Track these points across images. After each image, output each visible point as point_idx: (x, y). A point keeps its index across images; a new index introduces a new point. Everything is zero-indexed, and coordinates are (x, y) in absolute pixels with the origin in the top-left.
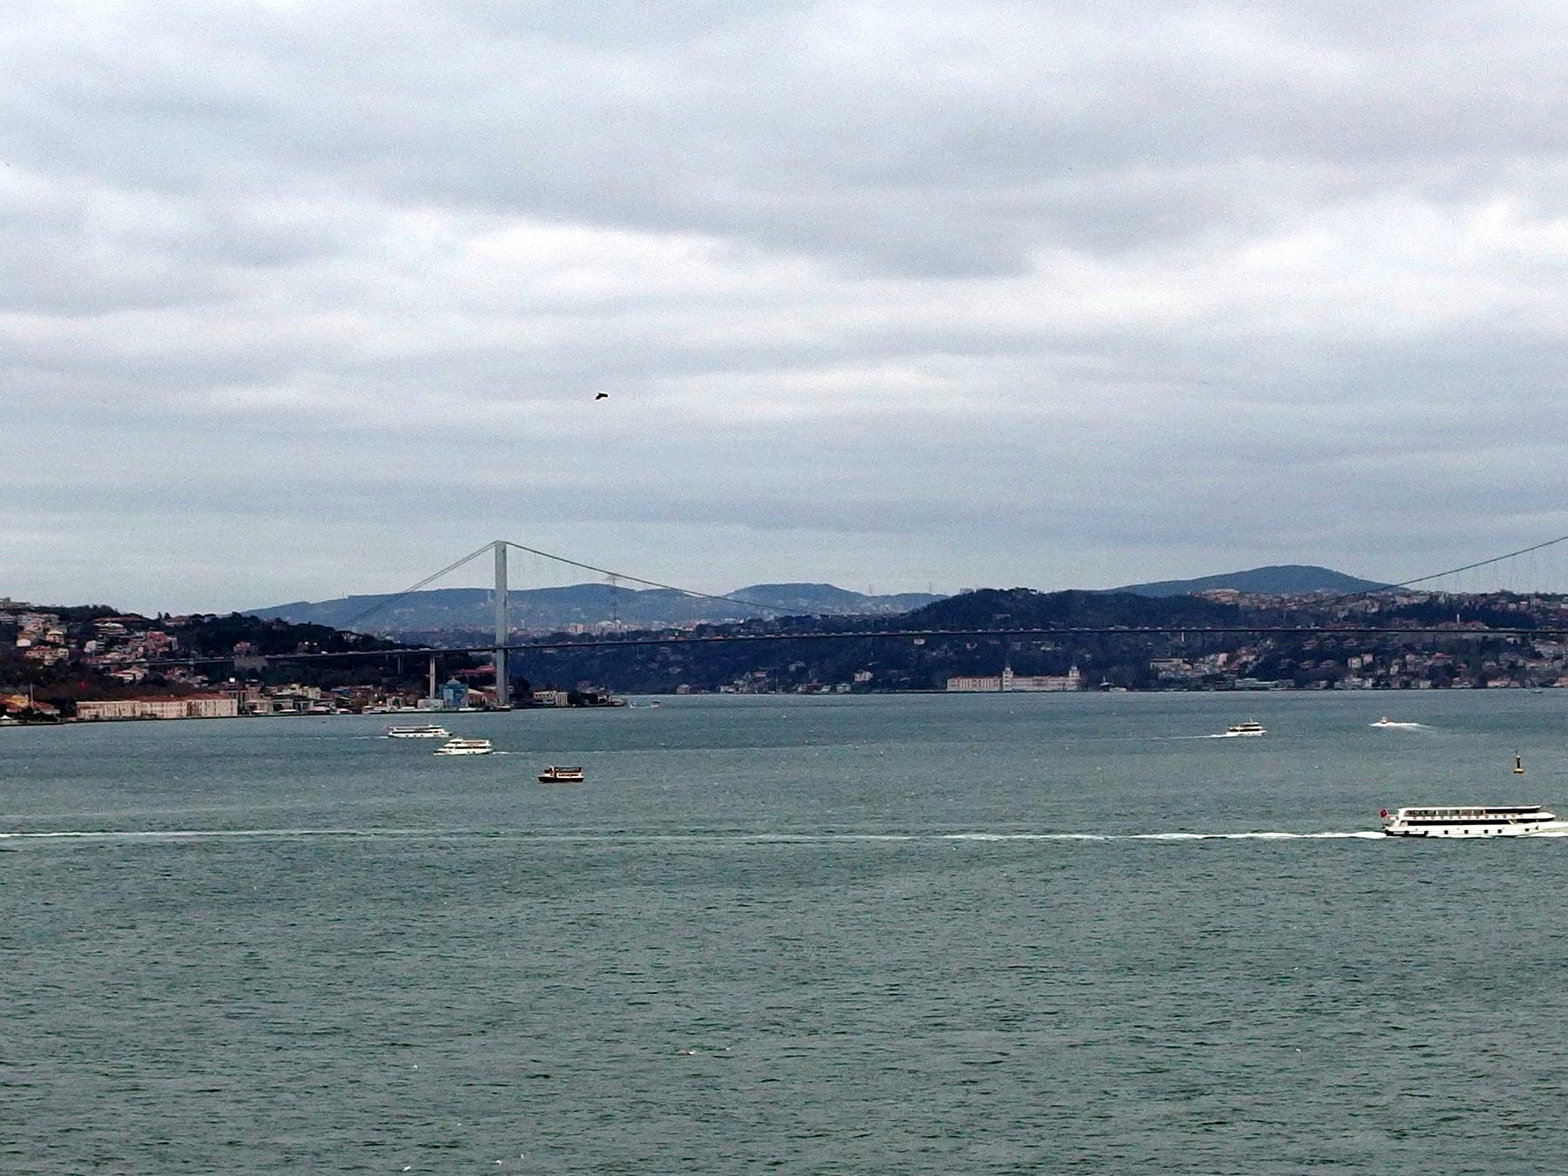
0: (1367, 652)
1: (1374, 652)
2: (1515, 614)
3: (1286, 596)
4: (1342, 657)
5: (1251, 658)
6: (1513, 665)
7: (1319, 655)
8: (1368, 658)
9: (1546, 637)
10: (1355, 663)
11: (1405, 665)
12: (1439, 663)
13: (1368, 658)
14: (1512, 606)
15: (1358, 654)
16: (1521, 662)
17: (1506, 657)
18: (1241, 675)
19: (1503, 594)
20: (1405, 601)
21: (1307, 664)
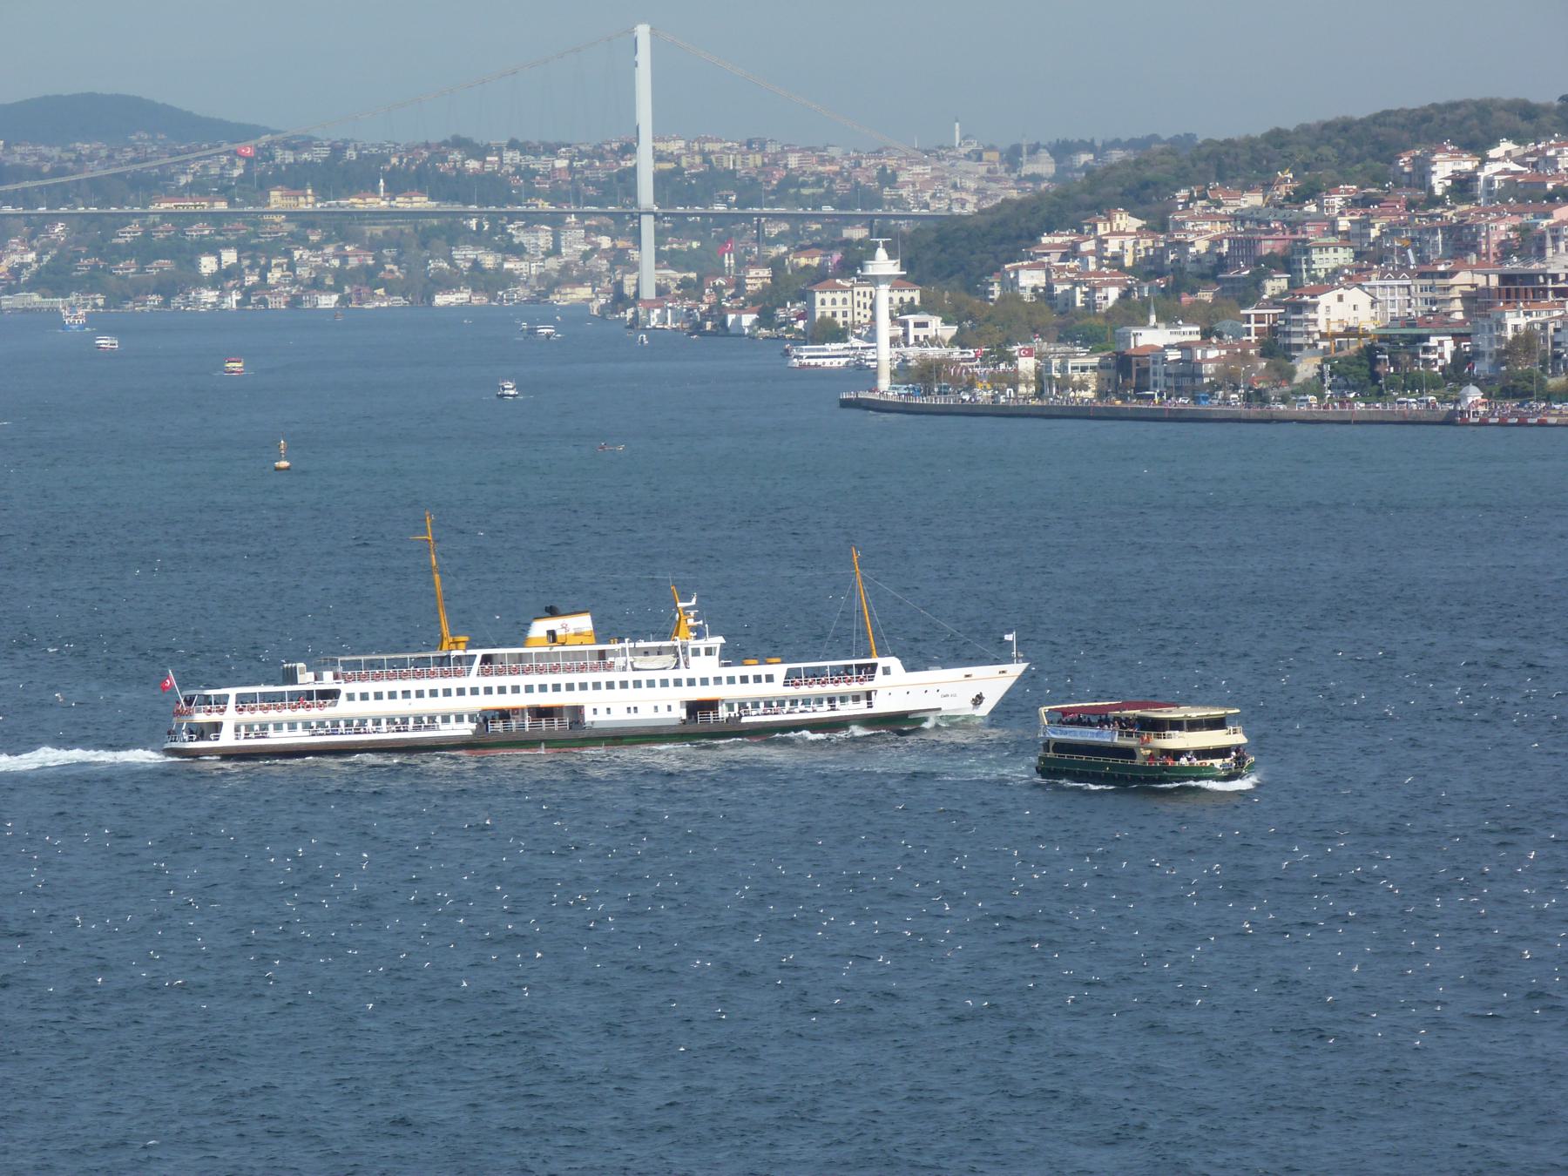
0: (227, 246)
1: (241, 246)
2: (478, 177)
3: (85, 148)
4: (187, 254)
5: (31, 257)
6: (476, 264)
7: (144, 250)
8: (229, 257)
9: (532, 220)
10: (208, 265)
11: (292, 267)
12: (353, 262)
13: (229, 257)
14: (473, 165)
15: (214, 250)
16: (489, 261)
17: (464, 255)
18: (11, 290)
19: (458, 143)
20: (289, 157)
21: (127, 268)
